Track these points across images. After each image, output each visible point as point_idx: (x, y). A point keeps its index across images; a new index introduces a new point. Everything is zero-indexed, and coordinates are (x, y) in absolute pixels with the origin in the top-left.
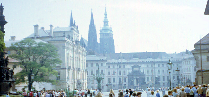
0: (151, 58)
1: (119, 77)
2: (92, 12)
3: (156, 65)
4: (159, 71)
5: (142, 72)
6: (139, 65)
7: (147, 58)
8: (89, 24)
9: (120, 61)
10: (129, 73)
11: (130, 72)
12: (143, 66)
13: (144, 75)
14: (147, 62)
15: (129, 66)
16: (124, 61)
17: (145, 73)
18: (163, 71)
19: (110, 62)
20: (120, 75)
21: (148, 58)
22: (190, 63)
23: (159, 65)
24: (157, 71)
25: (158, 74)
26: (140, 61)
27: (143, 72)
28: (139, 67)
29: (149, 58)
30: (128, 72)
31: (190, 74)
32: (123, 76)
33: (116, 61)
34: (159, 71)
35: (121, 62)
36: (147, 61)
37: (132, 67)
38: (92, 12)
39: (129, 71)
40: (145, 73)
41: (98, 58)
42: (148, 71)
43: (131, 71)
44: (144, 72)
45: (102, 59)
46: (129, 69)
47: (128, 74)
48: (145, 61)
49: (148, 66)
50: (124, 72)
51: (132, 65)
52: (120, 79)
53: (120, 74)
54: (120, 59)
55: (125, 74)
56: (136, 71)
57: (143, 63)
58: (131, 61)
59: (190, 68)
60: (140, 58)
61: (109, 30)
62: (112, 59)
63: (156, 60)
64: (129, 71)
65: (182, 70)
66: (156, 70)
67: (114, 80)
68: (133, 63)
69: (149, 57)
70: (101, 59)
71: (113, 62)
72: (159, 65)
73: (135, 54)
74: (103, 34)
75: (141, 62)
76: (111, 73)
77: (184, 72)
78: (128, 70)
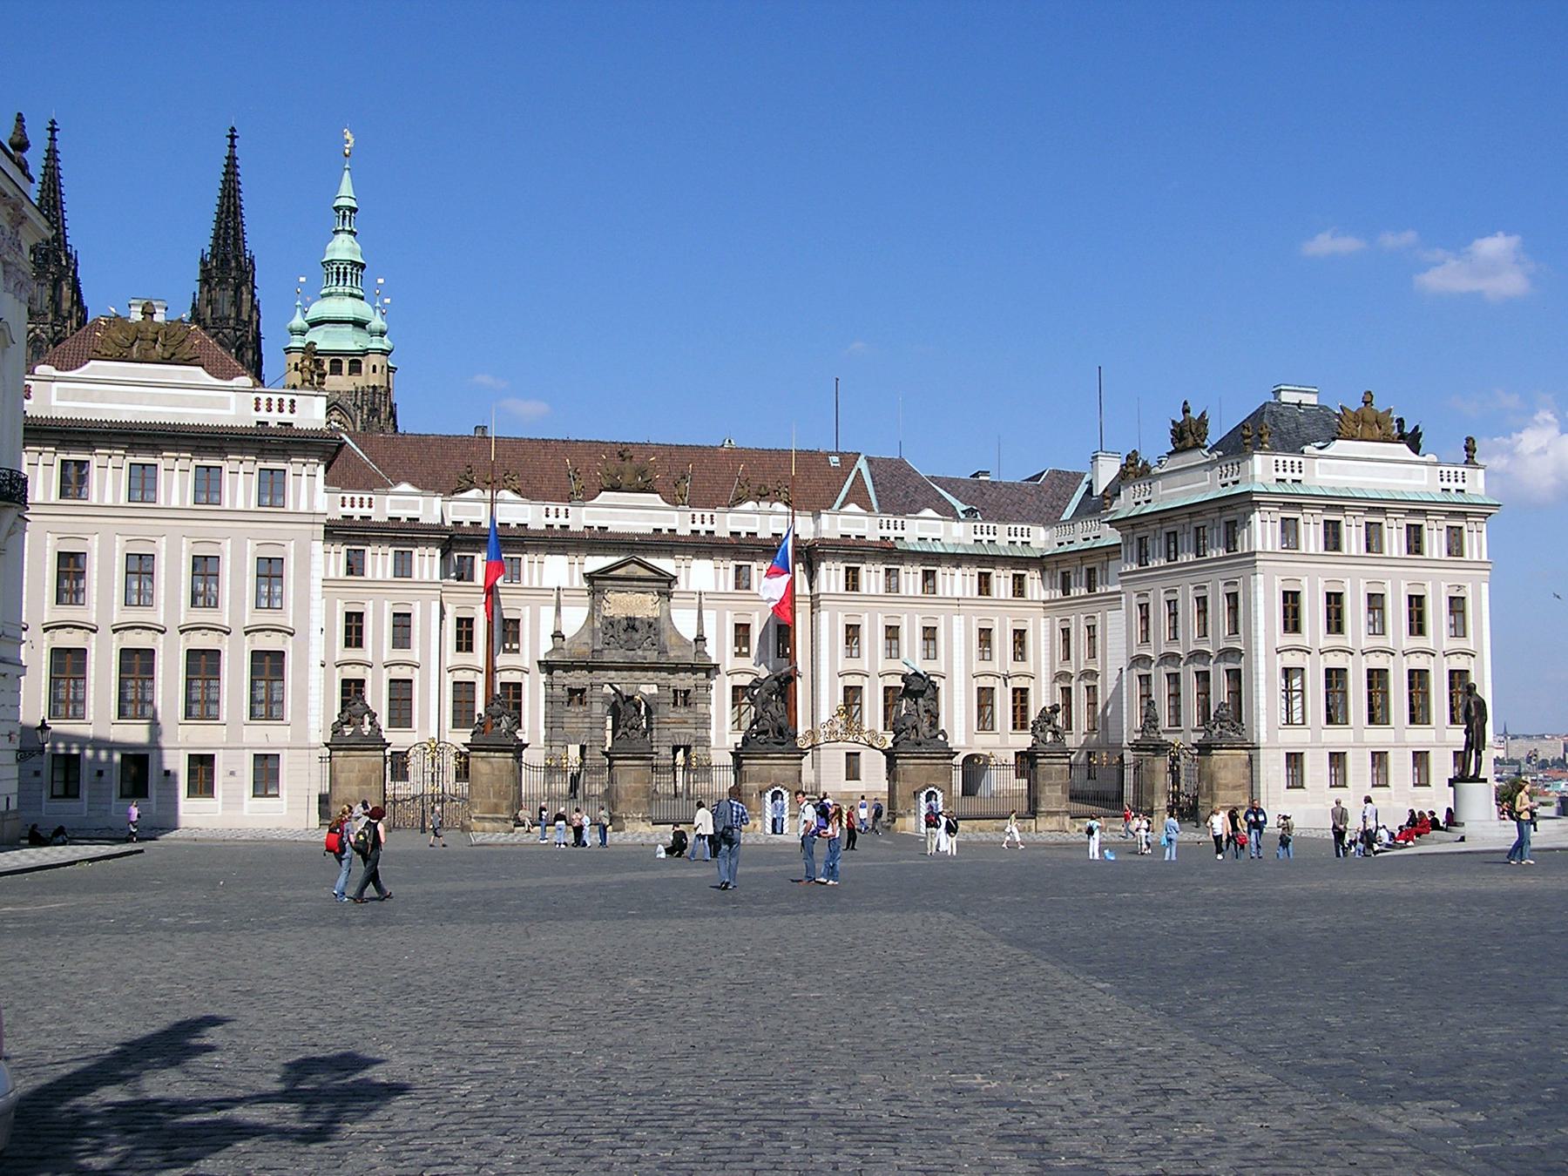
0: (780, 507)
1: (449, 680)
2: (232, 159)
3: (831, 575)
4: (852, 632)
5: (690, 635)
6: (666, 564)
7: (740, 500)
8: (202, 239)
9: (469, 509)
10: (557, 635)
11: (568, 633)
12: (701, 575)
13: (711, 670)
14: (741, 548)
15: (557, 570)
16: (517, 511)
17: (720, 648)
18: (892, 633)
19: (366, 511)
20: (464, 658)
23: (852, 581)
24: (831, 625)
25: (843, 664)
26: (680, 521)
27: (700, 639)
29: (764, 506)
30: (547, 630)
33: (430, 509)
34: (852, 632)
35: (483, 518)
36: (743, 530)
37: (590, 577)
38: (232, 159)
39: (558, 610)
40: (711, 649)
41: (229, 404)
43: (575, 618)
44: (710, 633)
45: (274, 418)
47: (546, 645)
49: (742, 580)
52: (463, 691)
53: (470, 648)
54: (474, 493)
56: (631, 624)
58: (580, 518)
59: (1233, 598)
61: (360, 324)
62: (396, 483)
64: (558, 610)
66: (824, 616)
67: (401, 692)
68: (597, 541)
69: (761, 496)
70: (263, 415)
71: (404, 514)
72: (852, 581)
73: (623, 452)
75: (684, 531)
76: (378, 630)
78: (548, 613)
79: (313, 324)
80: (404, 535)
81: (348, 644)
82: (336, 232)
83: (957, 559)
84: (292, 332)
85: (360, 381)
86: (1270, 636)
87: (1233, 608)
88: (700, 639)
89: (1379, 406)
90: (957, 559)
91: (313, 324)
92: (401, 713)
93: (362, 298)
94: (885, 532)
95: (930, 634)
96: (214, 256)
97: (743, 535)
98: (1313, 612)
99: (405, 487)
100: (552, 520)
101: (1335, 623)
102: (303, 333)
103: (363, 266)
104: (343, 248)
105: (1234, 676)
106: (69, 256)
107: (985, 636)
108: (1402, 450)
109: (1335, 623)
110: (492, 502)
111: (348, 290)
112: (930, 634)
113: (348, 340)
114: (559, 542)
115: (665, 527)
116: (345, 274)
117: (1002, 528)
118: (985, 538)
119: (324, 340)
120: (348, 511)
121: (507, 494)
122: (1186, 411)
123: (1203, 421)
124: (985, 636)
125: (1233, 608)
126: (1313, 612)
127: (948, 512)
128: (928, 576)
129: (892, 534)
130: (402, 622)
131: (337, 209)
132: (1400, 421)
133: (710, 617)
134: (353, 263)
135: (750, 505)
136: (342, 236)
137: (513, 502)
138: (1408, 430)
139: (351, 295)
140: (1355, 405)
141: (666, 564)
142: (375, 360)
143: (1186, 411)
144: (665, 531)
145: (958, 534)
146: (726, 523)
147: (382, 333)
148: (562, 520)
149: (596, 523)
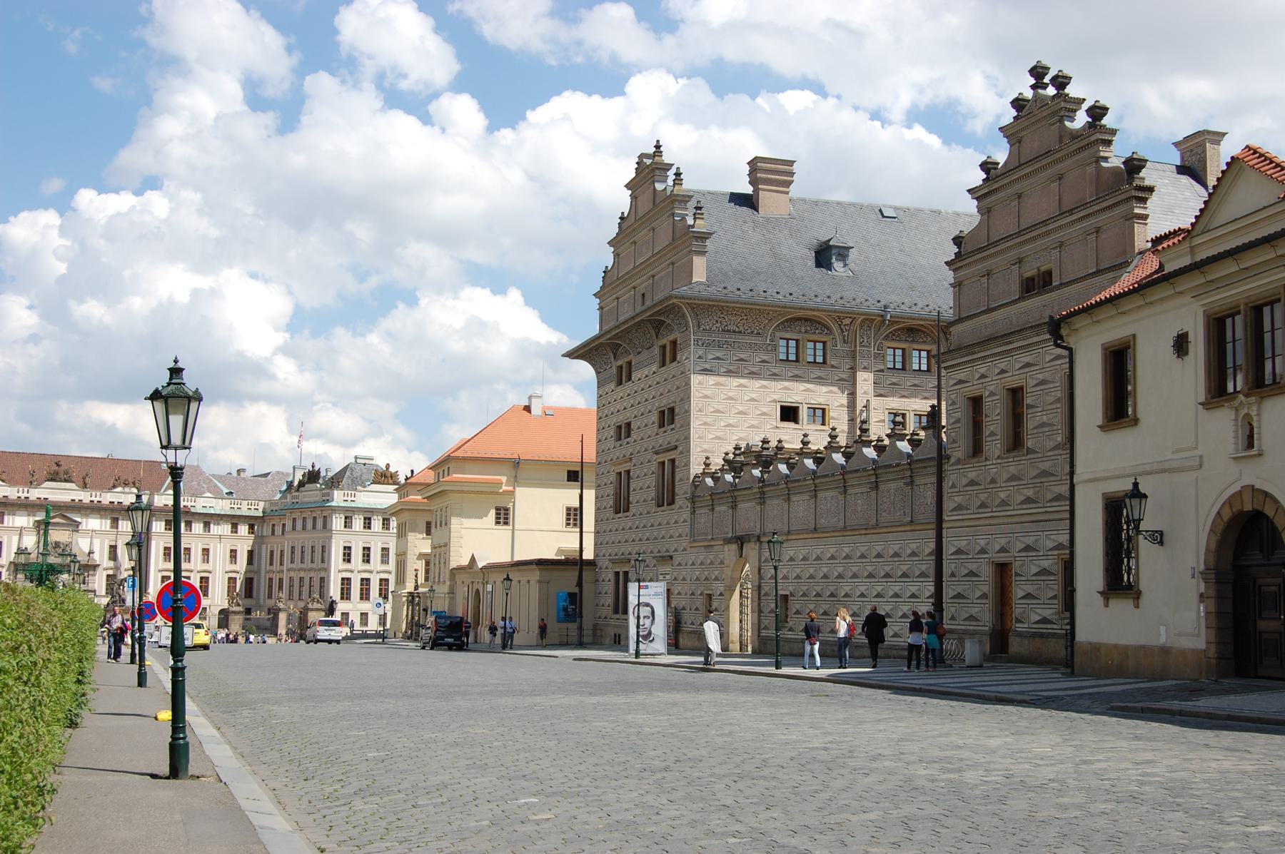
7: (114, 487)
12: (93, 523)
22: (325, 526)
26: (85, 497)
27: (91, 553)
28: (75, 526)
29: (127, 490)
31: (323, 574)
36: (116, 501)
40: (96, 556)
43: (30, 541)
44: (96, 548)
46: (21, 531)
49: (115, 522)
51: (40, 516)
57: (95, 509)
58: (35, 494)
60: (84, 486)
65: (272, 552)
66: (153, 543)
68: (43, 505)
69: (126, 484)
77: (292, 562)
78: (15, 539)
83: (220, 518)
86: (336, 564)
87: (323, 552)
88: (91, 553)
89: (392, 470)
95: (206, 552)
98: (357, 555)
101: (367, 559)
105: (322, 579)
107: (233, 553)
109: (367, 559)
112: (206, 552)
115: (77, 499)
117: (245, 503)
124: (233, 553)
125: (323, 552)
126: (357, 555)
127: (218, 495)
128: (207, 525)
133: (97, 542)
135: (119, 489)
145: (222, 506)
146: (107, 498)
148: (26, 495)
149: (42, 496)
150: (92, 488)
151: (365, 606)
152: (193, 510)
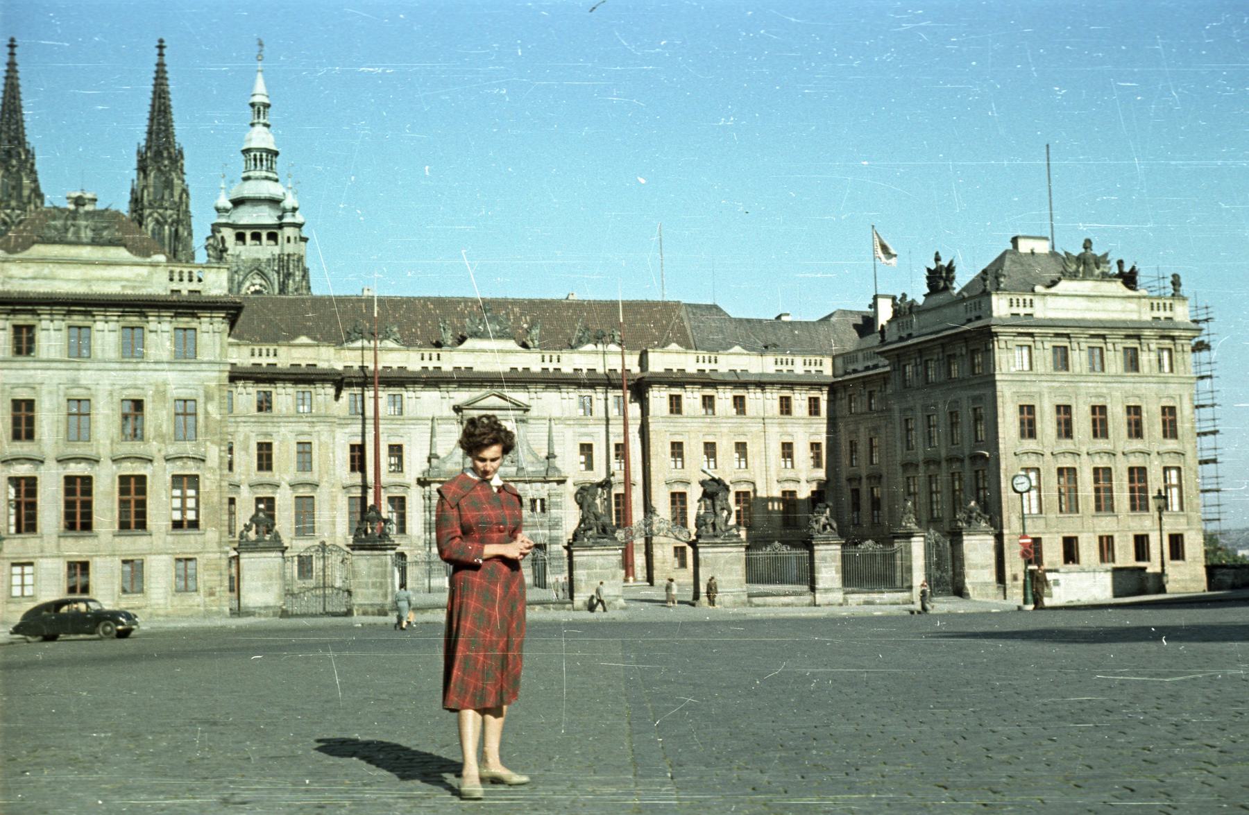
0: (613, 347)
2: (161, 66)
4: (677, 449)
7: (580, 342)
8: (139, 133)
19: (272, 360)
21: (588, 342)
23: (676, 405)
26: (533, 362)
27: (551, 456)
32: (385, 478)
34: (677, 449)
38: (161, 66)
41: (150, 277)
42: (586, 449)
48: (567, 369)
50: (396, 450)
55: (399, 467)
58: (450, 360)
61: (274, 202)
63: (659, 362)
67: (305, 507)
69: (599, 338)
72: (676, 405)
74: (233, 226)
75: (536, 368)
79: (238, 202)
80: (305, 377)
81: (260, 468)
82: (253, 125)
84: (218, 210)
85: (276, 250)
88: (551, 456)
89: (1097, 251)
90: (761, 384)
91: (238, 202)
92: (305, 525)
93: (277, 181)
94: (701, 366)
95: (741, 448)
96: (148, 148)
97: (585, 371)
99: (303, 339)
100: (426, 363)
102: (227, 211)
103: (276, 154)
104: (260, 138)
106: (27, 152)
108: (1118, 287)
110: (375, 349)
111: (264, 174)
113: (266, 216)
114: (434, 380)
116: (261, 160)
117: (799, 360)
118: (785, 368)
119: (246, 216)
120: (257, 360)
121: (389, 344)
122: (937, 259)
123: (950, 269)
124: (787, 450)
127: (750, 348)
129: (707, 367)
130: (305, 449)
131: (253, 105)
132: (1120, 263)
134: (268, 151)
136: (259, 128)
137: (391, 350)
138: (1127, 269)
139: (267, 178)
140: (1077, 250)
141: (520, 396)
142: (289, 232)
143: (937, 259)
144: (520, 369)
145: (764, 365)
147: (294, 210)
148: (435, 363)
150: (543, 347)
151: (1106, 525)
152: (714, 376)
